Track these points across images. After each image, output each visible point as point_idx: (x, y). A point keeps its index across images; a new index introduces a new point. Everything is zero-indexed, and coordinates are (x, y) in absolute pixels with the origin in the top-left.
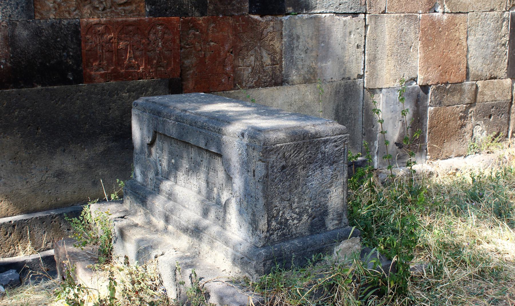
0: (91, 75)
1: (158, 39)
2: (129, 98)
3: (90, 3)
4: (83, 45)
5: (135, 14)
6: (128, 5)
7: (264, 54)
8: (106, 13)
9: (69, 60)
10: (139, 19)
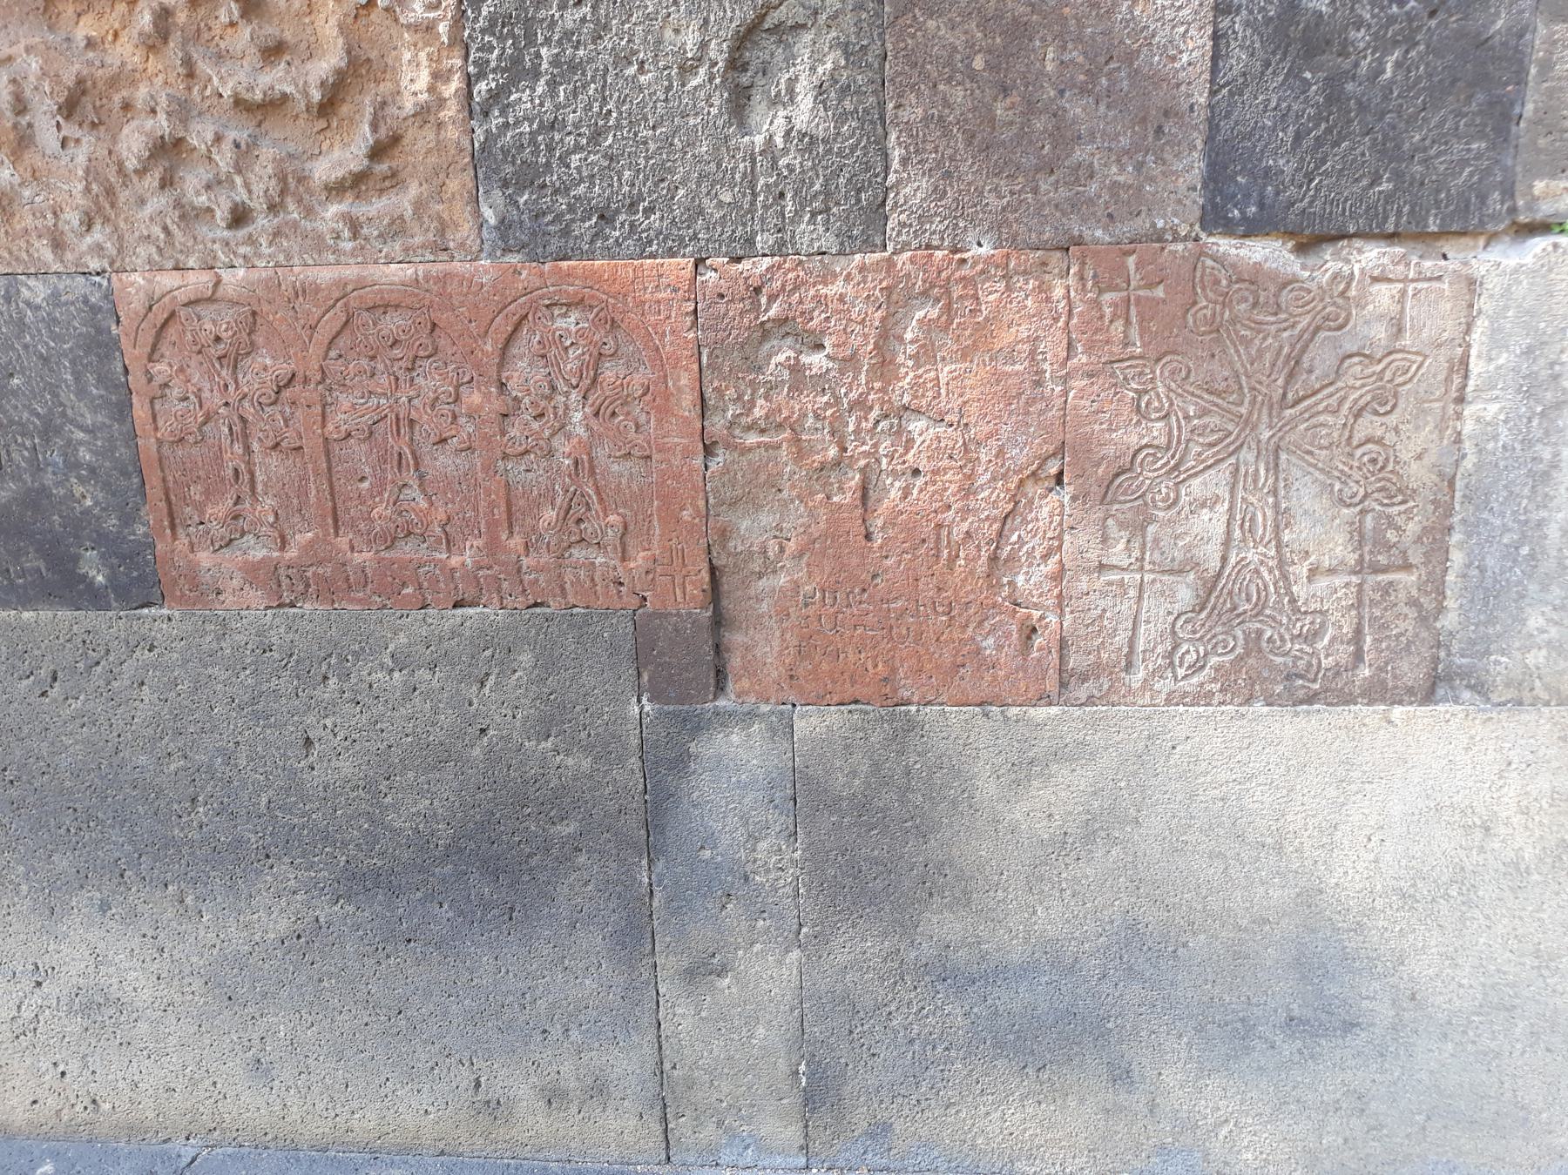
0: (194, 568)
2: (406, 698)
3: (166, 183)
4: (140, 411)
5: (418, 240)
6: (382, 191)
7: (1305, 495)
8: (251, 241)
9: (78, 490)
10: (436, 269)
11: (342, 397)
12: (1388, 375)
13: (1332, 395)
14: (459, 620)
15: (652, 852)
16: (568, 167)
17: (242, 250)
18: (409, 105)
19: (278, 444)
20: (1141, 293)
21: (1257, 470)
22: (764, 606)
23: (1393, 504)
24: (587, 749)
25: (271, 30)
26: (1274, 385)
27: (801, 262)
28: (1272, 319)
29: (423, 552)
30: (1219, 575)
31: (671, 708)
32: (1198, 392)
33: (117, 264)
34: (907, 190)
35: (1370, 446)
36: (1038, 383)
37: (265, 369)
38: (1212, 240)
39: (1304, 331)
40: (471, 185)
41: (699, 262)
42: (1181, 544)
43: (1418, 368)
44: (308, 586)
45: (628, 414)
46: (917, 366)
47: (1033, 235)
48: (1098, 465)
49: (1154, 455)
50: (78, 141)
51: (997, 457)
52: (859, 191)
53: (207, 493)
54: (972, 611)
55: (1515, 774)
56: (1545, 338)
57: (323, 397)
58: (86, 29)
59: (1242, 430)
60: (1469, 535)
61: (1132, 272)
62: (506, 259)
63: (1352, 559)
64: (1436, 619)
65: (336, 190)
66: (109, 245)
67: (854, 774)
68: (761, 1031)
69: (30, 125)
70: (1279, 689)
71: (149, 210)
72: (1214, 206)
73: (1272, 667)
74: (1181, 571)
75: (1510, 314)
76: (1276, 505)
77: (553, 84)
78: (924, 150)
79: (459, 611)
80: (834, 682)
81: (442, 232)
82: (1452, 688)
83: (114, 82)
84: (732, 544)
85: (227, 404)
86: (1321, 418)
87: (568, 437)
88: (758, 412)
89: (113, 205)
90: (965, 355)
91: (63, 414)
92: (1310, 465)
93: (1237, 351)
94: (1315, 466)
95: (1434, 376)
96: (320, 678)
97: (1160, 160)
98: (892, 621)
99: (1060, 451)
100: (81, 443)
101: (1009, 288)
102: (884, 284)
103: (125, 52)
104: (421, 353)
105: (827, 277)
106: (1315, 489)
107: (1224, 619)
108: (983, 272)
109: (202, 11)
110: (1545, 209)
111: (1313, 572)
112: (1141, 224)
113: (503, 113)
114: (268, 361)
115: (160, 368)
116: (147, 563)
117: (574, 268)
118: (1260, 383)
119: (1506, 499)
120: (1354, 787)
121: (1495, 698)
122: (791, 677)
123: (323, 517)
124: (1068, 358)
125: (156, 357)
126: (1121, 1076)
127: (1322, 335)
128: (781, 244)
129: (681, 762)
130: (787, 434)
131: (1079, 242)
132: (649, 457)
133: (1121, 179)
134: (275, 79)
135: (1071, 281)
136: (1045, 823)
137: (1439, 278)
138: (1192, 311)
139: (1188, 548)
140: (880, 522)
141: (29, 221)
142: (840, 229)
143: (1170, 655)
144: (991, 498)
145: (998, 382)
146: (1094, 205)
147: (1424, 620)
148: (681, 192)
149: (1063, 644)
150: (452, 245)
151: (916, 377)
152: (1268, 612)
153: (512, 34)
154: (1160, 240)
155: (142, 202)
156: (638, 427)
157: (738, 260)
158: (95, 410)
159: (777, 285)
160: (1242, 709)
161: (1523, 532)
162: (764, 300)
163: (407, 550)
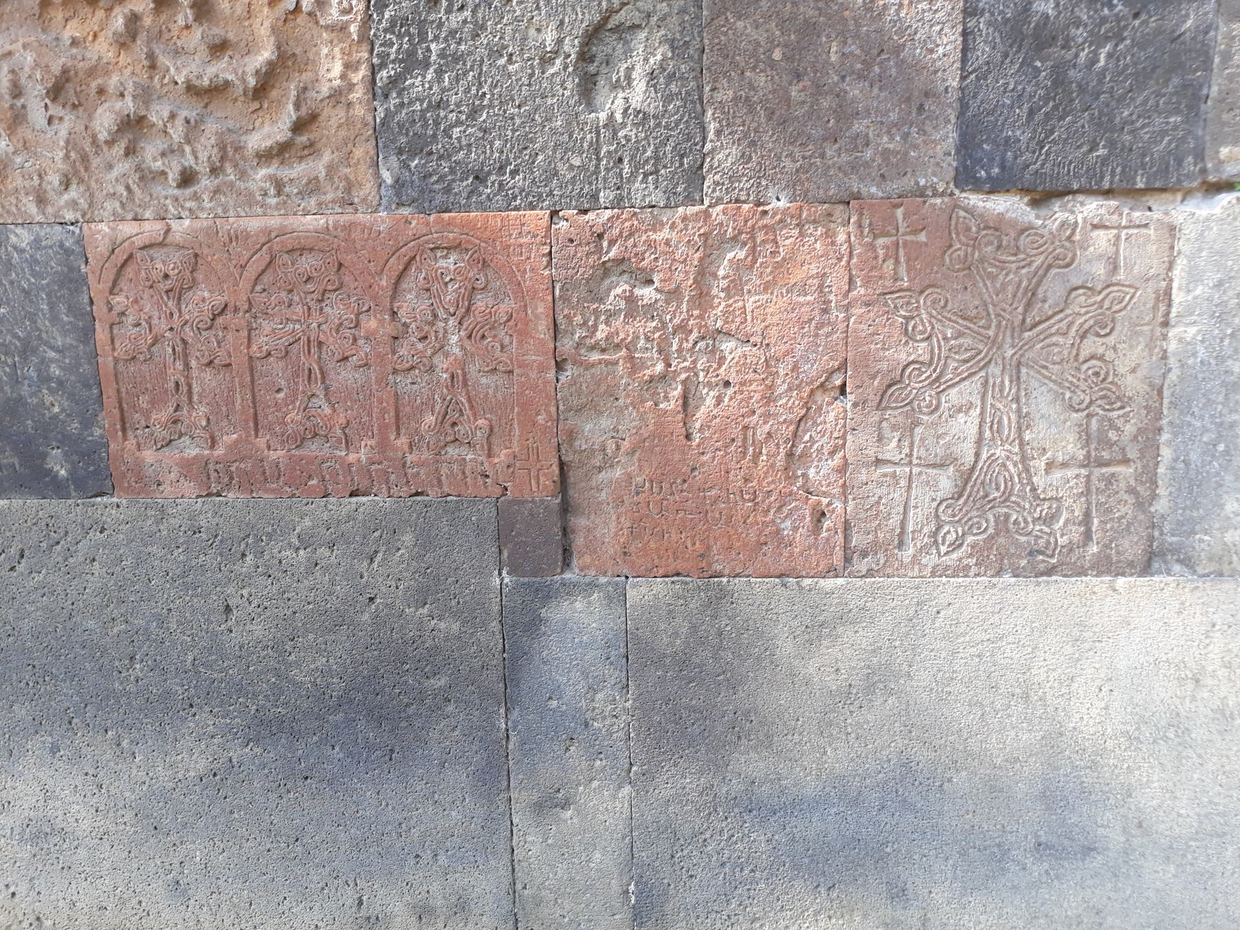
0: (139, 464)
1: (441, 314)
2: (309, 572)
3: (130, 152)
4: (101, 334)
5: (330, 196)
6: (301, 158)
7: (1042, 402)
8: (196, 197)
9: (48, 399)
11: (265, 323)
12: (1107, 304)
13: (1061, 321)
14: (354, 506)
15: (509, 703)
16: (451, 137)
17: (188, 204)
18: (325, 90)
19: (211, 362)
20: (908, 238)
21: (1003, 382)
22: (603, 494)
23: (1113, 410)
24: (456, 615)
25: (217, 31)
26: (1015, 314)
27: (635, 213)
28: (1013, 259)
29: (327, 450)
30: (973, 468)
31: (526, 579)
32: (954, 318)
33: (88, 217)
34: (720, 156)
35: (1093, 362)
36: (825, 311)
37: (204, 300)
38: (964, 195)
39: (1039, 268)
40: (373, 152)
41: (554, 214)
42: (942, 442)
43: (1131, 298)
44: (231, 478)
45: (495, 336)
46: (729, 297)
47: (821, 192)
48: (874, 377)
49: (919, 369)
50: (61, 119)
51: (792, 371)
52: (682, 157)
53: (153, 402)
54: (772, 499)
55: (1218, 634)
56: (1232, 274)
57: (249, 323)
58: (72, 30)
59: (991, 348)
60: (1176, 435)
61: (900, 221)
62: (400, 211)
63: (1081, 454)
64: (1151, 504)
65: (265, 156)
66: (82, 201)
67: (676, 634)
68: (597, 856)
69: (24, 107)
70: (1023, 563)
71: (115, 173)
72: (965, 167)
73: (1018, 545)
74: (942, 465)
75: (1204, 254)
76: (1019, 410)
77: (440, 73)
78: (734, 124)
79: (354, 499)
80: (660, 558)
81: (348, 190)
82: (1165, 562)
83: (92, 72)
84: (577, 443)
85: (171, 329)
86: (1054, 339)
87: (447, 355)
88: (600, 335)
89: (86, 169)
90: (767, 287)
91: (39, 338)
92: (1045, 377)
93: (985, 285)
94: (1049, 379)
95: (1144, 305)
96: (239, 556)
97: (922, 132)
98: (708, 507)
99: (843, 367)
100: (52, 360)
101: (801, 234)
102: (702, 231)
103: (102, 49)
104: (329, 287)
105: (656, 226)
106: (1050, 397)
107: (978, 505)
108: (781, 221)
109: (163, 17)
110: (1230, 170)
111: (1050, 466)
112: (907, 183)
113: (400, 94)
114: (206, 294)
115: (119, 300)
116: (101, 459)
117: (454, 218)
118: (1004, 310)
119: (1204, 405)
120: (1087, 646)
121: (1200, 570)
122: (625, 553)
123: (246, 421)
124: (849, 291)
125: (116, 291)
126: (898, 894)
127: (1054, 271)
128: (620, 199)
129: (533, 625)
130: (623, 352)
131: (858, 196)
132: (511, 372)
133: (891, 146)
134: (221, 69)
135: (851, 228)
136: (833, 676)
137: (1146, 226)
138: (949, 252)
139: (948, 445)
140: (698, 425)
141: (19, 182)
142: (667, 187)
143: (934, 534)
144: (788, 405)
145: (793, 310)
146: (869, 167)
147: (1140, 505)
148: (540, 158)
149: (847, 527)
150: (356, 200)
151: (728, 306)
152: (1013, 499)
153: (408, 33)
154: (922, 195)
155: (110, 167)
156: (502, 347)
157: (585, 212)
158: (65, 333)
159: (616, 232)
160: (994, 580)
161: (1219, 432)
162: (605, 244)
163: (313, 449)
